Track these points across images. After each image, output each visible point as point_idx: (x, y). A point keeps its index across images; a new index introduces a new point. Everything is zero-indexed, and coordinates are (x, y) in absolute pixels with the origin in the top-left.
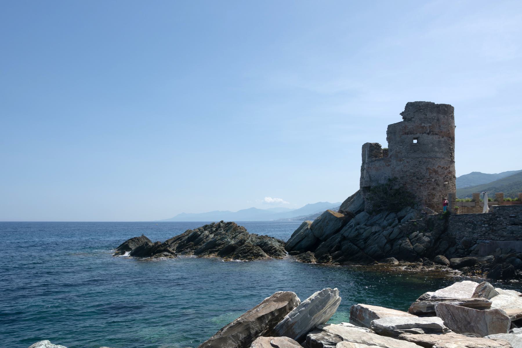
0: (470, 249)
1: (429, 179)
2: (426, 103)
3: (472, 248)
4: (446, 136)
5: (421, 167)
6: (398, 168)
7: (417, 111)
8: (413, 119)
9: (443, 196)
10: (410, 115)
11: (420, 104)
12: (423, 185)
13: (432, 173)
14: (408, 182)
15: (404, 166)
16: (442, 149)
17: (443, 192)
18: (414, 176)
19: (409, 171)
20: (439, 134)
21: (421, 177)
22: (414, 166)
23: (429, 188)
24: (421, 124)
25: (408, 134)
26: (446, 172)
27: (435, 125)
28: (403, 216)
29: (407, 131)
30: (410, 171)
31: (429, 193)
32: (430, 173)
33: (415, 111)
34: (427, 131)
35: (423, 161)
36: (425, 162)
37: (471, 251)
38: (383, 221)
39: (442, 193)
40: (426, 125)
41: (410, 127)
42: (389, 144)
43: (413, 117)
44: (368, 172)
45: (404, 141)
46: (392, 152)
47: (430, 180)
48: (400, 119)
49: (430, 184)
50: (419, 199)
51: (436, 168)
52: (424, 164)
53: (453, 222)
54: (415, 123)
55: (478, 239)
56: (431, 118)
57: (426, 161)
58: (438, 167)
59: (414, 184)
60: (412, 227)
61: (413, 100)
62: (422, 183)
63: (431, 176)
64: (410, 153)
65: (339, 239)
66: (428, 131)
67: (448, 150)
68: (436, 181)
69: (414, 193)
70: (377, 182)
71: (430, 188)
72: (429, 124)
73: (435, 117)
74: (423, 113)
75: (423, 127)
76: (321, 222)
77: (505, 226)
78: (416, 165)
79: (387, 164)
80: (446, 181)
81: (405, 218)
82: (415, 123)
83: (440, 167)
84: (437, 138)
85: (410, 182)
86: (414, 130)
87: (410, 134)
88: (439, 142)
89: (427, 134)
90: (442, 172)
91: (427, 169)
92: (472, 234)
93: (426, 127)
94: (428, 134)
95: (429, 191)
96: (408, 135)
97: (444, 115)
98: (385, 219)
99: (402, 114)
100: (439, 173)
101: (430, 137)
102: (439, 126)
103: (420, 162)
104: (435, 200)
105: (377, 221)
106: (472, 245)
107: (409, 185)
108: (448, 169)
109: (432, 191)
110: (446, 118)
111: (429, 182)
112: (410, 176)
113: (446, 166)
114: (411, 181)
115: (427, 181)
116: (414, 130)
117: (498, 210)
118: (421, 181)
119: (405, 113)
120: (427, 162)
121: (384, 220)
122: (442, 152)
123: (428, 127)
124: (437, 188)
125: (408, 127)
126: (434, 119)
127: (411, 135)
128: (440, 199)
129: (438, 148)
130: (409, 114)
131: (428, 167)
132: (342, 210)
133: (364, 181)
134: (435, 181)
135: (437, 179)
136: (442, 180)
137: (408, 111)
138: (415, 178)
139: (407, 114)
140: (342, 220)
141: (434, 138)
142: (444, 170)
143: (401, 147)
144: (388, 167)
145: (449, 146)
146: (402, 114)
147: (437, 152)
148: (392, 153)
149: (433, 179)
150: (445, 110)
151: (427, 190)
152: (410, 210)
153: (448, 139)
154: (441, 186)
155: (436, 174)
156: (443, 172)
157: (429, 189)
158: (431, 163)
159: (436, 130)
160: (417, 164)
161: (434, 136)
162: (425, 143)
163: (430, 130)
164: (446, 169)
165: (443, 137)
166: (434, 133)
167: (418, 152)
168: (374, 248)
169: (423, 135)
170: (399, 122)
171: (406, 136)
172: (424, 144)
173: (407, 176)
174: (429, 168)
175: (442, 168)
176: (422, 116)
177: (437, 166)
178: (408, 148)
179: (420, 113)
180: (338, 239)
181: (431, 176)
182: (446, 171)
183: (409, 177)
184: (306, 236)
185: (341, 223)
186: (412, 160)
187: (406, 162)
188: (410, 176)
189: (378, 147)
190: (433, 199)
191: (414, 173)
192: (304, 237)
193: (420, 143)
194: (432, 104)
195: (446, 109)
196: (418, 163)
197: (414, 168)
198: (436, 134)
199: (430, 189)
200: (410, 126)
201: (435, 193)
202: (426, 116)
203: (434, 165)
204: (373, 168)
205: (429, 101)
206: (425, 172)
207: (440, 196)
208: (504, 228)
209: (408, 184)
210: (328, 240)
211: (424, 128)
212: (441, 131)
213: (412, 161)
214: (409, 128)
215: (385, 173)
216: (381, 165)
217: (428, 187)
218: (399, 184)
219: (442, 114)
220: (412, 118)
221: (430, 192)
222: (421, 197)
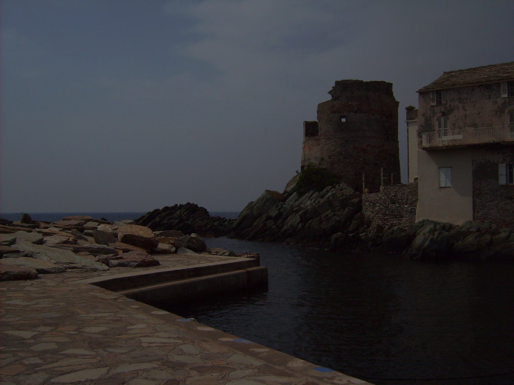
30: (338, 150)
43: (340, 96)
48: (329, 98)
61: (340, 79)
66: (356, 109)
70: (309, 161)
76: (259, 202)
77: (388, 205)
94: (356, 112)
96: (336, 114)
98: (309, 198)
99: (330, 92)
105: (303, 200)
117: (384, 189)
130: (336, 93)
132: (286, 190)
143: (329, 126)
144: (318, 146)
146: (330, 92)
148: (321, 132)
152: (330, 189)
170: (328, 101)
183: (336, 156)
202: (353, 94)
208: (387, 207)
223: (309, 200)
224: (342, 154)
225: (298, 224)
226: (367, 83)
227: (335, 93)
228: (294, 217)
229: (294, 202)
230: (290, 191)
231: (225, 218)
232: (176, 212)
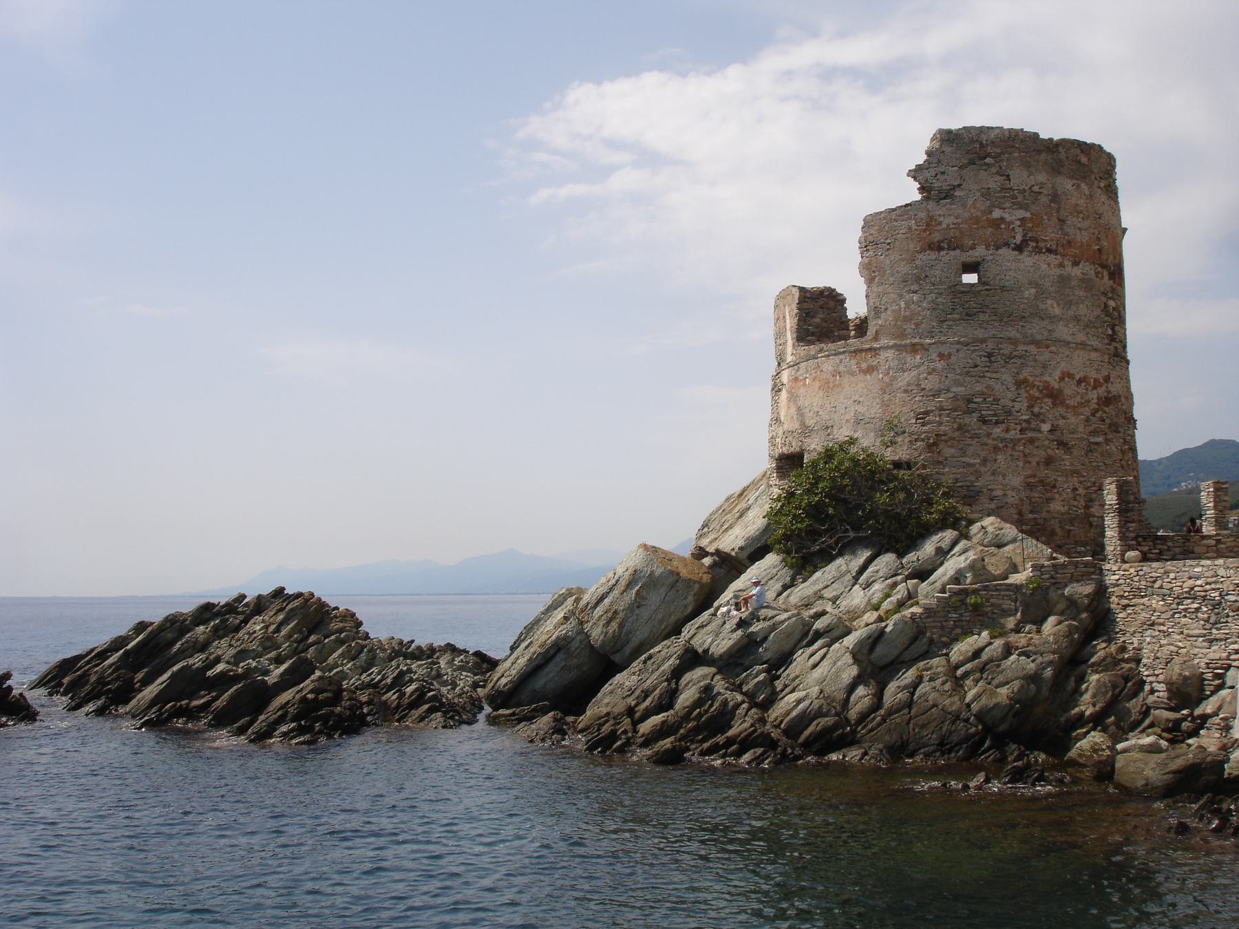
0: (1198, 712)
1: (1028, 421)
2: (1007, 133)
3: (1208, 707)
4: (1087, 261)
5: (994, 375)
6: (905, 379)
7: (972, 162)
8: (957, 193)
9: (1084, 492)
10: (946, 177)
11: (984, 137)
12: (1006, 446)
13: (1039, 398)
14: (944, 435)
15: (930, 373)
16: (1074, 308)
17: (1085, 474)
18: (969, 412)
19: (948, 390)
20: (1060, 250)
21: (995, 415)
22: (965, 370)
24: (991, 212)
25: (940, 249)
26: (1093, 395)
27: (1045, 217)
28: (930, 567)
29: (937, 237)
30: (954, 389)
32: (1032, 401)
33: (965, 162)
34: (1014, 237)
35: (1003, 355)
36: (1010, 358)
37: (1205, 718)
38: (851, 589)
39: (1081, 479)
40: (1007, 217)
41: (946, 221)
42: (868, 287)
43: (959, 185)
44: (793, 397)
45: (927, 276)
46: (883, 315)
47: (1033, 426)
48: (911, 193)
49: (1031, 441)
50: (992, 500)
51: (1053, 379)
52: (1006, 362)
53: (1127, 594)
54: (964, 206)
55: (1230, 666)
56: (1027, 188)
57: (1014, 353)
58: (1062, 379)
59: (969, 441)
60: (961, 615)
62: (1003, 440)
63: (1036, 410)
64: (950, 323)
65: (673, 661)
66: (1019, 239)
67: (1098, 312)
68: (1058, 433)
69: (973, 478)
71: (1034, 460)
72: (1021, 214)
73: (1042, 185)
74: (994, 170)
75: (996, 224)
78: (976, 366)
79: (864, 366)
80: (1095, 432)
81: (932, 578)
82: (964, 206)
83: (1071, 376)
84: (1052, 266)
85: (957, 434)
86: (961, 233)
87: (949, 249)
88: (1063, 280)
89: (1013, 250)
90: (1078, 399)
91: (1020, 384)
92: (1204, 644)
93: (1011, 223)
94: (1019, 248)
95: (1030, 472)
96: (942, 253)
97: (1077, 179)
99: (916, 173)
100: (1067, 402)
101: (1027, 260)
102: (1058, 219)
103: (989, 355)
104: (1056, 506)
105: (827, 587)
106: (1208, 693)
107: (952, 447)
108: (1104, 388)
109: (1043, 472)
110: (1087, 192)
111: (1030, 434)
112: (954, 410)
113: (1093, 375)
114: (960, 428)
115: (1021, 430)
116: (961, 233)
118: (998, 430)
119: (927, 171)
120: (1020, 357)
121: (853, 586)
122: (1076, 319)
123: (1018, 223)
124: (1063, 460)
125: (940, 223)
126: (1040, 193)
127: (952, 253)
128: (1076, 503)
129: (1059, 305)
130: (943, 173)
131: (1021, 377)
133: (780, 433)
134: (1050, 431)
135: (1061, 422)
136: (1081, 429)
137: (939, 161)
138: (972, 420)
139: (937, 174)
140: (697, 586)
141: (1044, 266)
142: (1087, 389)
145: (1103, 299)
146: (916, 173)
147: (1053, 319)
149: (1043, 421)
150: (1079, 162)
151: (1021, 464)
153: (1097, 273)
154: (1075, 452)
155: (1054, 404)
156: (1082, 398)
157: (1030, 463)
158: (1035, 361)
159: (1050, 235)
160: (978, 362)
161: (1043, 257)
162: (1007, 284)
163: (1024, 236)
164: (1094, 388)
165: (1076, 264)
166: (1042, 245)
167: (981, 316)
168: (806, 703)
169: (1000, 252)
170: (907, 205)
171: (933, 255)
172: (1003, 288)
173: (942, 409)
174: (1025, 381)
175: (1079, 382)
176: (994, 183)
177: (1057, 374)
178: (943, 304)
179: (986, 170)
180: (670, 662)
181: (1036, 410)
182: (1095, 391)
183: (948, 416)
184: (559, 649)
185: (690, 598)
186: (958, 347)
187: (934, 356)
188: (954, 410)
189: (832, 304)
190: (1048, 500)
191: (969, 401)
192: (552, 652)
193: (988, 285)
194: (1030, 137)
195: (1084, 160)
196: (983, 359)
197: (967, 379)
198: (1049, 251)
199: (1034, 464)
200: (948, 217)
201: (1056, 480)
202: (1009, 180)
203: (1044, 367)
204: (814, 379)
205: (1016, 126)
206: (1010, 395)
207: (1075, 489)
209: (946, 441)
210: (634, 664)
211: (1003, 226)
212: (1069, 242)
213: (958, 351)
214: (944, 226)
215: (855, 401)
216: (841, 368)
217: (1025, 456)
218: (910, 441)
219: (1072, 178)
220: (954, 188)
221: (1034, 476)
222: (999, 493)
223: (857, 586)
224: (971, 405)
225: (851, 688)
226: (1053, 147)
227: (937, 174)
228: (822, 659)
229: (780, 594)
230: (741, 548)
231: (413, 641)
232: (246, 621)
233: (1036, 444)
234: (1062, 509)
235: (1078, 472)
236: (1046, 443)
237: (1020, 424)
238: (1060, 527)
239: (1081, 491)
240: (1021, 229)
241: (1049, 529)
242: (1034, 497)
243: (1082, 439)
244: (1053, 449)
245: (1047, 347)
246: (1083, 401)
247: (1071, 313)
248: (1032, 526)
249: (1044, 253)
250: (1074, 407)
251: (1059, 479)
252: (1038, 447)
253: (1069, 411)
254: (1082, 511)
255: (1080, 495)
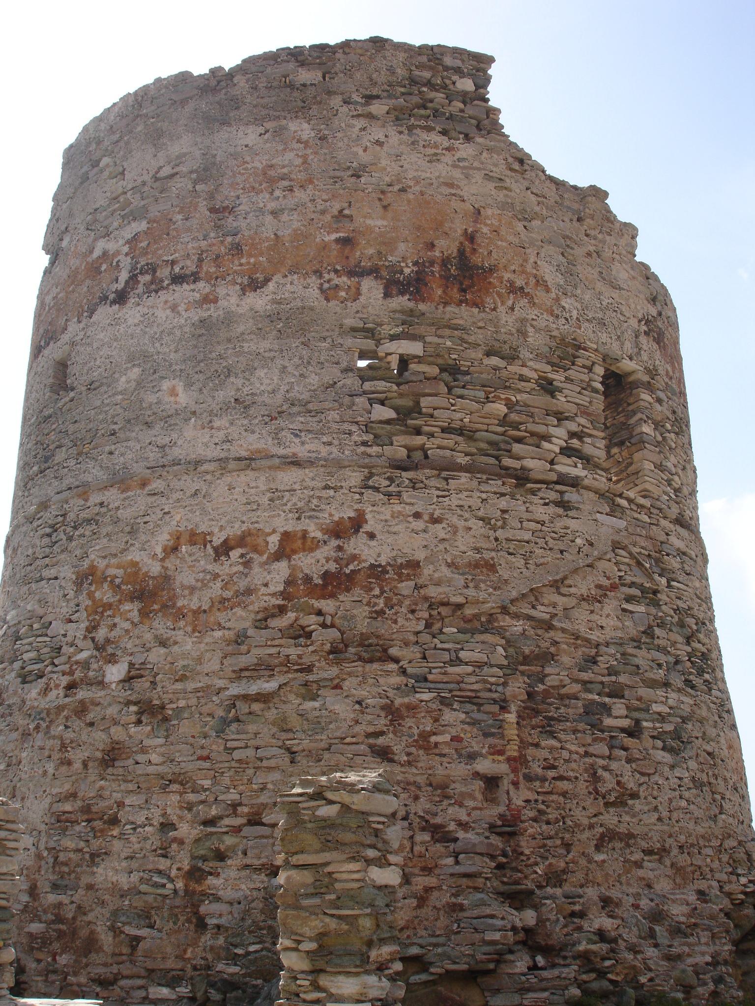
1: (86, 665)
13: (110, 606)
23: (70, 755)
31: (68, 807)
49: (82, 709)
58: (173, 550)
68: (142, 685)
71: (77, 756)
100: (180, 604)
120: (88, 521)
122: (241, 404)
124: (144, 751)
129: (189, 385)
134: (128, 679)
135: (157, 655)
141: (162, 314)
149: (112, 659)
154: (185, 728)
155: (145, 614)
156: (225, 587)
158: (116, 521)
175: (223, 550)
181: (101, 633)
190: (95, 857)
198: (178, 279)
199: (77, 765)
201: (120, 804)
203: (133, 532)
207: (167, 826)
233: (90, 717)
234: (124, 881)
235: (181, 780)
236: (112, 711)
237: (71, 673)
238: (112, 928)
239: (186, 830)
240: (129, 259)
241: (84, 933)
242: (66, 850)
243: (206, 691)
244: (125, 726)
245: (144, 484)
246: (228, 594)
247: (226, 394)
248: (49, 923)
249: (167, 288)
250: (197, 612)
251: (127, 802)
252: (91, 724)
253: (182, 623)
254: (180, 885)
255: (181, 842)
